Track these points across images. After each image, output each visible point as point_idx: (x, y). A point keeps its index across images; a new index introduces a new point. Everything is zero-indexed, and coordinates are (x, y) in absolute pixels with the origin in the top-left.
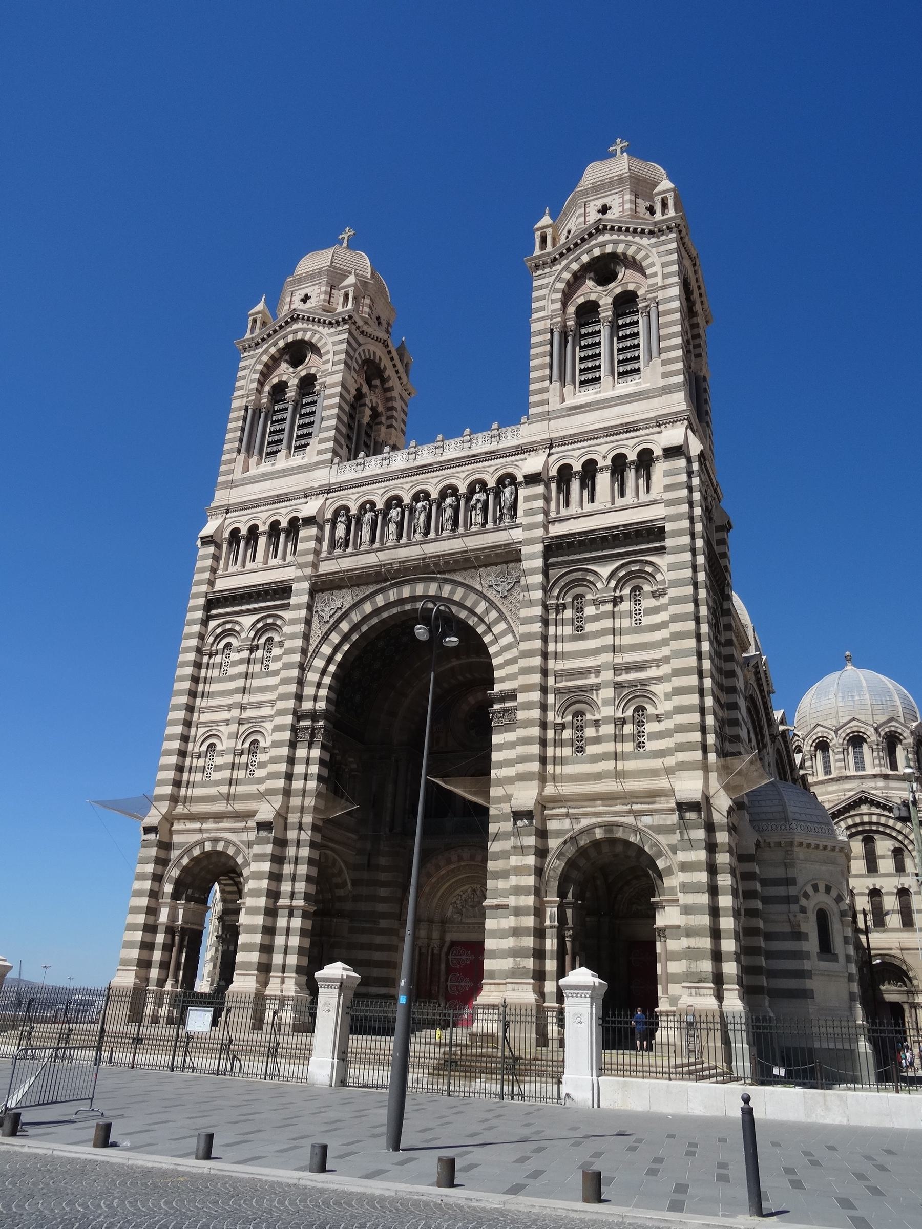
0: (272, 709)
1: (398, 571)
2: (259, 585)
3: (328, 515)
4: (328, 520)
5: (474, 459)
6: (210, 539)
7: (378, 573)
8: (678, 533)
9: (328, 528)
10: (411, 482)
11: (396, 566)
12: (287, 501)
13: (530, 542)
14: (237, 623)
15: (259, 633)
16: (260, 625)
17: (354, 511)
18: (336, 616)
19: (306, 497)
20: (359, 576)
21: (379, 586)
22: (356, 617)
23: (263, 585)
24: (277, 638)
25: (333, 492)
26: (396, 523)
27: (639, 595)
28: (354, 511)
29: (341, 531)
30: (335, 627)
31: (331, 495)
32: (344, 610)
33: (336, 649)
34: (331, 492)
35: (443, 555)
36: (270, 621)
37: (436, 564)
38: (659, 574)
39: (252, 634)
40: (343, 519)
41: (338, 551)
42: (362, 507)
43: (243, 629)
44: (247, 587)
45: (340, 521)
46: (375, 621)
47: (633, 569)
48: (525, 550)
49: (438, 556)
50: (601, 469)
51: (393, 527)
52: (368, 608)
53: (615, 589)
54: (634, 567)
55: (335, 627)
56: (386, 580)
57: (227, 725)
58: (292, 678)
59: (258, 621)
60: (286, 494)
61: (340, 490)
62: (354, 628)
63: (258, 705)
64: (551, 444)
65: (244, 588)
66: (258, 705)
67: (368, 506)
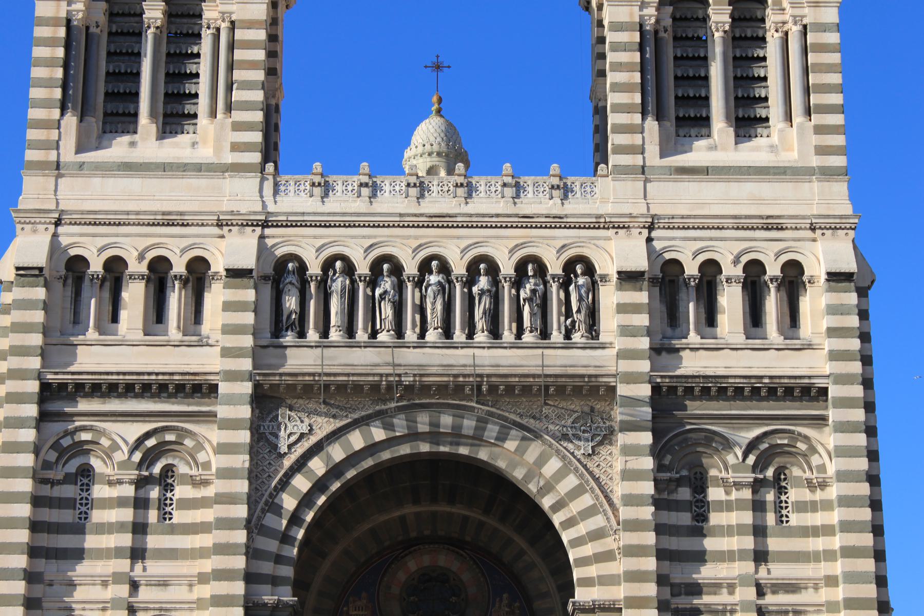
0: (191, 591)
1: (409, 388)
2: (149, 374)
3: (269, 270)
4: (265, 278)
5: (527, 222)
6: (37, 272)
7: (375, 387)
8: (845, 403)
9: (267, 289)
10: (416, 238)
11: (407, 380)
12: (183, 225)
13: (631, 378)
14: (103, 433)
15: (150, 457)
16: (151, 442)
17: (314, 269)
18: (300, 450)
19: (220, 224)
20: (342, 388)
21: (378, 408)
22: (337, 453)
23: (157, 374)
24: (182, 469)
25: (273, 226)
26: (393, 303)
27: (785, 479)
28: (314, 269)
29: (291, 303)
30: (300, 465)
31: (268, 231)
32: (313, 440)
33: (306, 501)
34: (268, 226)
35: (489, 376)
36: (170, 437)
37: (479, 387)
38: (817, 455)
39: (137, 457)
40: (293, 279)
41: (289, 338)
42: (328, 265)
43: (115, 447)
44: (124, 374)
45: (290, 283)
46: (368, 463)
47: (779, 442)
48: (623, 390)
49: (481, 376)
50: (728, 280)
51: (387, 311)
52: (357, 440)
53: (754, 468)
54: (780, 438)
55: (300, 465)
56: (392, 399)
57: (104, 609)
58: (236, 545)
59: (148, 435)
60: (182, 213)
61: (287, 226)
62: (335, 471)
63: (164, 584)
64: (652, 223)
65: (118, 373)
66: (164, 584)
67: (338, 264)
